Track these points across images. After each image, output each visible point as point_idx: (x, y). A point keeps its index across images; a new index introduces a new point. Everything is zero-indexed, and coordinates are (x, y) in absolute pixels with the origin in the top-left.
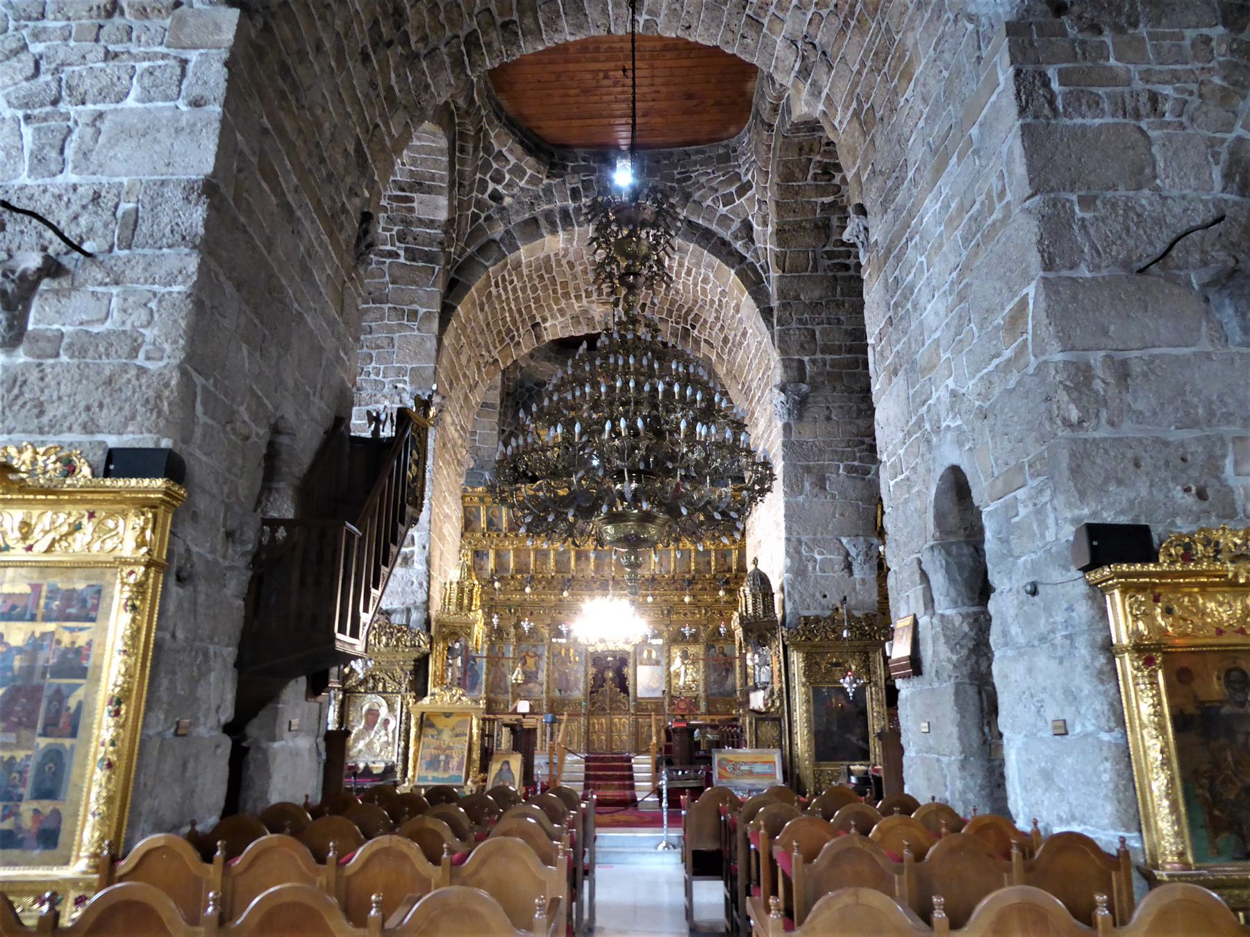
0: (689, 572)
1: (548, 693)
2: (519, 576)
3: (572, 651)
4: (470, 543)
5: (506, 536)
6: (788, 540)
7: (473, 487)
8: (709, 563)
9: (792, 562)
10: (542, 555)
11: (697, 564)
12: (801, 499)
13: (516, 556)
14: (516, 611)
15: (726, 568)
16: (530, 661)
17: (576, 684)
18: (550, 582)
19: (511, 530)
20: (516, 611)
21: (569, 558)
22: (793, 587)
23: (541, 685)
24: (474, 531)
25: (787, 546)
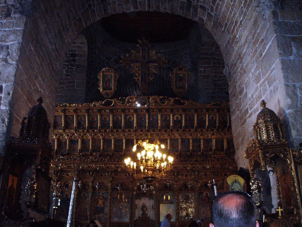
0: (189, 150)
1: (110, 219)
2: (94, 154)
3: (123, 196)
4: (68, 135)
5: (88, 131)
6: (287, 86)
7: (70, 104)
8: (199, 146)
9: (292, 101)
10: (107, 142)
11: (193, 146)
12: (292, 58)
13: (93, 142)
14: (93, 174)
15: (208, 149)
16: (100, 202)
17: (126, 215)
18: (111, 157)
19: (90, 128)
20: (93, 174)
21: (122, 144)
22: (295, 120)
23: (106, 215)
24: (71, 129)
25: (287, 90)
